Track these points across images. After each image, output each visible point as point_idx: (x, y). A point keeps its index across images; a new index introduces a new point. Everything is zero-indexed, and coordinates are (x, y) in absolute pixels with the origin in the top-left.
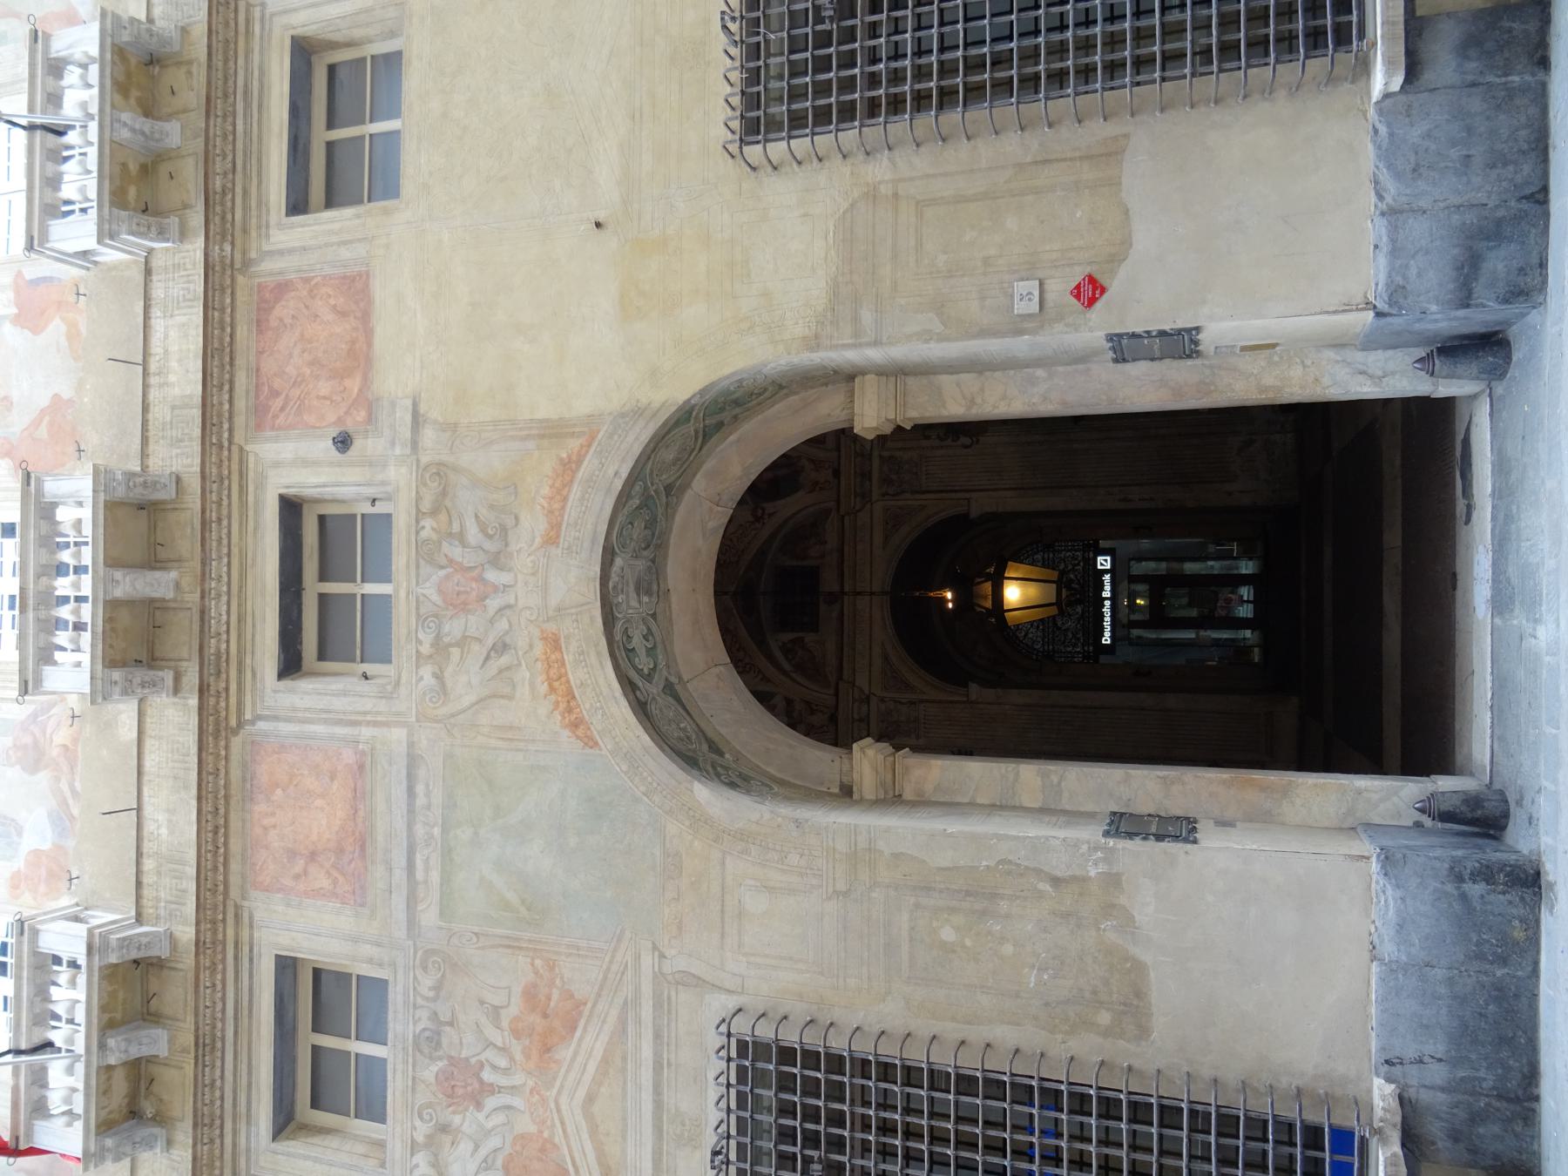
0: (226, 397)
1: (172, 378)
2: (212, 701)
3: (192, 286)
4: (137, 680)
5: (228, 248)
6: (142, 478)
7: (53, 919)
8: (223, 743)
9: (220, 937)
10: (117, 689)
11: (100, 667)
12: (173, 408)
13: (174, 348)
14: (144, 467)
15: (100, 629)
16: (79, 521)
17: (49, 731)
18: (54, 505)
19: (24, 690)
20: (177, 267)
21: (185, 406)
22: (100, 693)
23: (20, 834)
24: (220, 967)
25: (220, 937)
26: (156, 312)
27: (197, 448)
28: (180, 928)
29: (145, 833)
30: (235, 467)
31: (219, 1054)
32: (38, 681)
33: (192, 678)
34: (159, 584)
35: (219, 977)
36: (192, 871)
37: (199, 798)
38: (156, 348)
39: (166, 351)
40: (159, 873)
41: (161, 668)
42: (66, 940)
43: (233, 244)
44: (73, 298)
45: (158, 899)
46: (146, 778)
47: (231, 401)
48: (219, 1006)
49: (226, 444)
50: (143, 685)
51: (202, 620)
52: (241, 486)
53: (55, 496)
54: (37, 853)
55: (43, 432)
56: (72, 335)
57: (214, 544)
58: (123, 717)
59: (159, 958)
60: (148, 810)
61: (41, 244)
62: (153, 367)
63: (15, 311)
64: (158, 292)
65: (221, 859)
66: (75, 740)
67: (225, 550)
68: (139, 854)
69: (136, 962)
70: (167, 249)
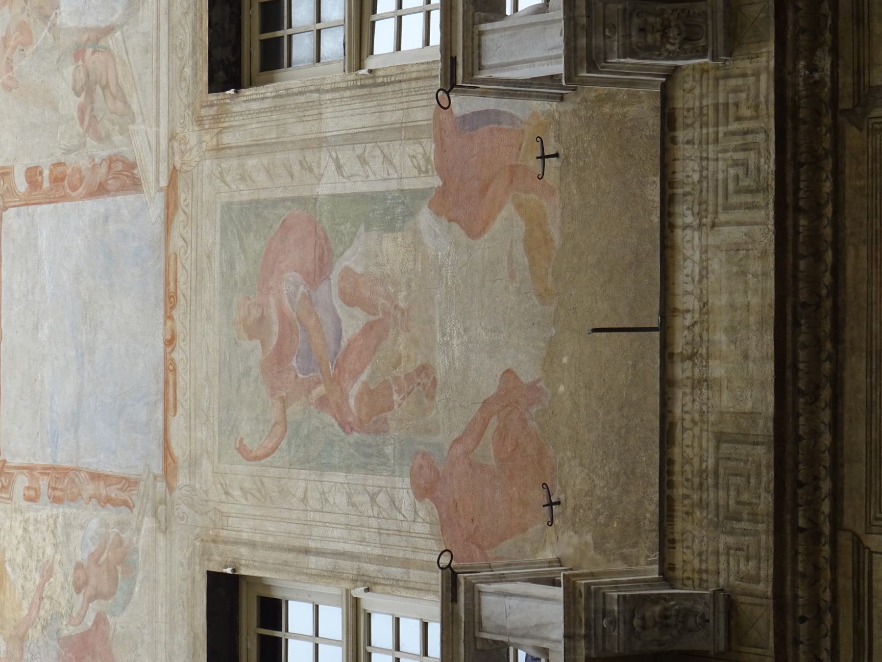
0: (826, 416)
1: (717, 370)
3: (752, 156)
5: (826, 63)
12: (720, 438)
13: (719, 301)
14: (667, 574)
20: (723, 111)
21: (742, 438)
26: (684, 215)
27: (767, 540)
30: (846, 584)
38: (686, 299)
43: (835, 51)
44: (535, 165)
47: (836, 426)
49: (826, 529)
52: (858, 632)
53: (501, 630)
55: (487, 451)
56: (536, 241)
61: (469, 75)
62: (680, 342)
63: (437, 182)
64: (688, 170)
70: (704, 71)
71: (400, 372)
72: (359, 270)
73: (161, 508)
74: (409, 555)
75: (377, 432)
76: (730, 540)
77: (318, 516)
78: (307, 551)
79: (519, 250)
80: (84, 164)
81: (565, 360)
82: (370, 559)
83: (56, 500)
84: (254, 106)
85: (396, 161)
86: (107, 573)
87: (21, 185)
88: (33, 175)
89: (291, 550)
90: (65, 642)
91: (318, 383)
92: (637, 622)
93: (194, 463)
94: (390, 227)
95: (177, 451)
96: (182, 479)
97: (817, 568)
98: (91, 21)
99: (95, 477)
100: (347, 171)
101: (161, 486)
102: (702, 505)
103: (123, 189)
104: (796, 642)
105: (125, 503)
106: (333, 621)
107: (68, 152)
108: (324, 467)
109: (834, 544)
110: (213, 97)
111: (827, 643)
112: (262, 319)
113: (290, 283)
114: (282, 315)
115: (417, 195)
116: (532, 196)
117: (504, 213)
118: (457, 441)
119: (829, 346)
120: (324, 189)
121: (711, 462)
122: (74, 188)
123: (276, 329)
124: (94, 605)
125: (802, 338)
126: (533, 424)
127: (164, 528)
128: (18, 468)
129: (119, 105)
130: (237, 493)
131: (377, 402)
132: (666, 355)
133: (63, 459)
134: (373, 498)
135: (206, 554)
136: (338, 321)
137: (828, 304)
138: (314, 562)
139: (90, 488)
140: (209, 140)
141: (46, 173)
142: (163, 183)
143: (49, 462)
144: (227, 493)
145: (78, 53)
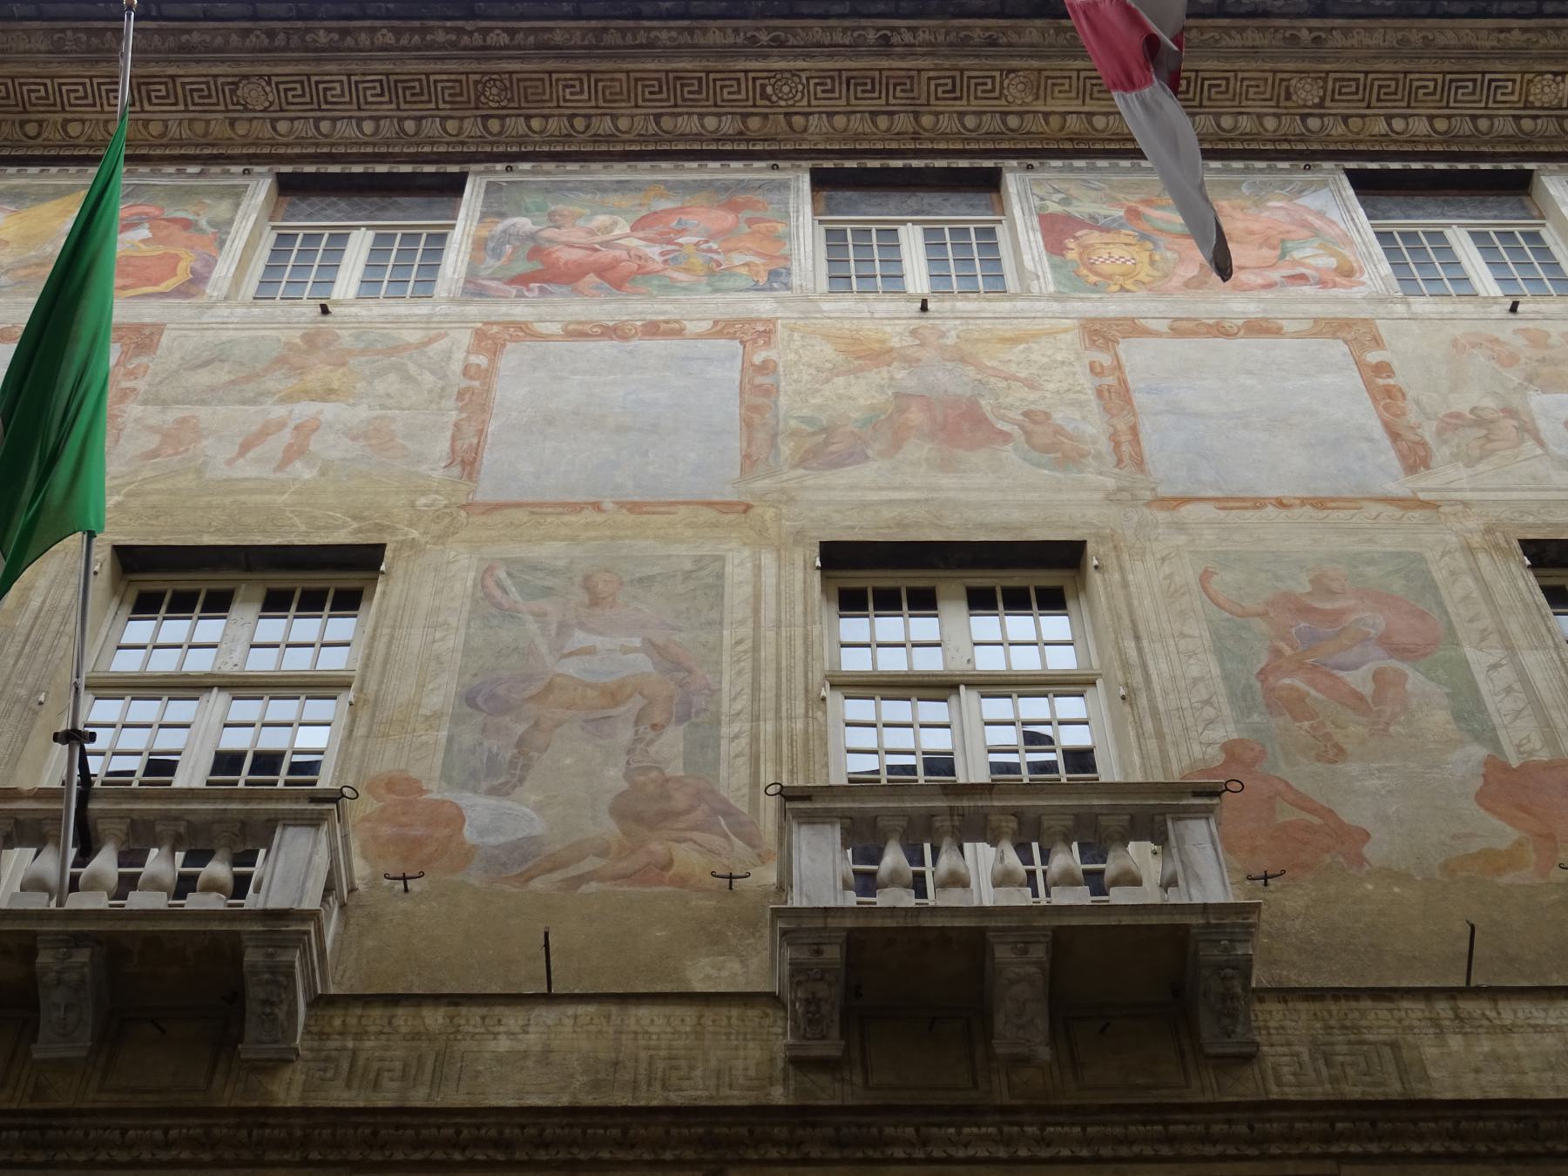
0: (1437, 1147)
2: (780, 1132)
4: (822, 990)
6: (1235, 990)
7: (333, 851)
8: (689, 1154)
9: (272, 1156)
10: (804, 955)
11: (849, 923)
12: (1394, 1046)
13: (1518, 1044)
14: (1262, 994)
15: (926, 922)
16: (1136, 881)
17: (697, 836)
18: (1160, 838)
19: (788, 795)
21: (1403, 1070)
22: (798, 927)
23: (493, 791)
24: (206, 1157)
25: (272, 1156)
27: (1320, 1092)
28: (300, 1078)
29: (498, 1010)
31: (19, 1157)
32: (810, 818)
33: (828, 1092)
34: (1019, 1025)
35: (185, 1155)
36: (419, 1098)
37: (572, 1111)
38: (1509, 1012)
39: (1508, 1030)
40: (415, 1036)
41: (844, 1034)
42: (289, 873)
45: (360, 1036)
46: (614, 1009)
47: (1429, 1157)
48: (121, 1156)
49: (1335, 1149)
50: (812, 1001)
51: (954, 1110)
53: (1181, 839)
54: (457, 818)
55: (1288, 814)
56: (1494, 861)
57: (1118, 1130)
58: (734, 966)
59: (240, 1039)
60: (547, 1015)
62: (1468, 1006)
65: (439, 1155)
66: (682, 881)
67: (1106, 1152)
68: (455, 1000)
69: (236, 997)
71: (1330, 728)
72: (1408, 687)
73: (1127, 496)
74: (1168, 738)
75: (1268, 706)
76: (1306, 1057)
77: (1172, 648)
78: (1137, 638)
79: (1475, 846)
80: (1412, 417)
81: (1396, 890)
82: (1152, 700)
83: (1099, 393)
84: (1521, 584)
85: (1519, 723)
86: (1052, 446)
87: (1373, 357)
88: (1382, 369)
89: (1133, 622)
90: (973, 403)
91: (1292, 647)
92: (1229, 971)
93: (1180, 527)
94: (1458, 717)
95: (1186, 511)
96: (1161, 516)
97: (1298, 1140)
98: (1542, 424)
99: (1134, 430)
100: (1494, 675)
101: (1148, 495)
102: (1328, 1028)
103: (1403, 457)
104: (1229, 1122)
105: (1120, 462)
106: (1063, 660)
107: (1418, 403)
108: (1220, 653)
109: (1324, 1156)
110: (1516, 544)
111: (1232, 1151)
112: (1331, 593)
113: (1376, 621)
114: (1339, 614)
115: (1495, 742)
116: (1534, 857)
117: (1509, 829)
118: (1287, 784)
119: (1501, 1150)
120: (1470, 653)
121: (1369, 1037)
122: (1386, 407)
123: (1328, 606)
124: (1016, 431)
125: (1506, 1125)
126: (1328, 859)
127: (1111, 498)
128: (1116, 355)
129: (1477, 453)
130: (1167, 569)
131: (1294, 706)
132: (1451, 993)
133: (1139, 399)
134: (1208, 702)
135: (1101, 539)
136: (1356, 667)
137: (1538, 1148)
138: (1130, 645)
139: (1122, 426)
140: (1476, 540)
141: (1391, 381)
142: (1421, 496)
143: (1132, 386)
144: (1163, 559)
145: (1510, 412)
